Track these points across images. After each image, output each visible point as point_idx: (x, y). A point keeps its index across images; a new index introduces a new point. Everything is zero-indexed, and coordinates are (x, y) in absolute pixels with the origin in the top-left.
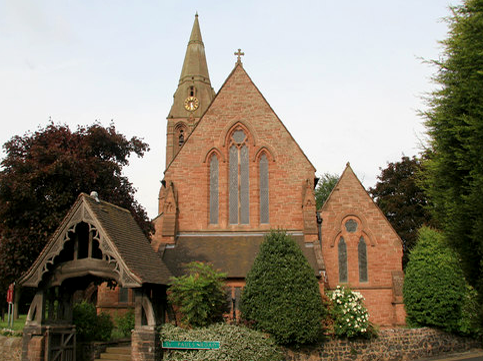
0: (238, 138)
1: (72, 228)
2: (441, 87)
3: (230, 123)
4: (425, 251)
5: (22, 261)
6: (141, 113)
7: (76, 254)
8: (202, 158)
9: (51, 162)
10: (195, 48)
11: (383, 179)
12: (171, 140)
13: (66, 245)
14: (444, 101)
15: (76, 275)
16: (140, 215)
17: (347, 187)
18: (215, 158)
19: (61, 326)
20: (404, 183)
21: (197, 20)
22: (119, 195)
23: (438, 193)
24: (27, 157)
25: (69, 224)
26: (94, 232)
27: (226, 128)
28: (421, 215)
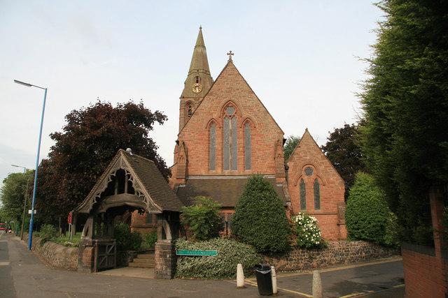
0: (230, 112)
1: (113, 173)
2: (371, 77)
3: (223, 101)
4: (360, 188)
5: (78, 196)
6: (162, 94)
7: (116, 190)
8: (205, 125)
9: (99, 128)
10: (200, 50)
11: (331, 139)
12: (183, 113)
13: (110, 184)
14: (374, 87)
15: (116, 205)
16: (161, 164)
17: (306, 145)
18: (213, 125)
19: (105, 240)
20: (346, 142)
21: (201, 31)
22: (146, 150)
23: (369, 149)
24: (82, 125)
25: (111, 170)
26: (129, 176)
27: (221, 105)
28: (358, 164)
